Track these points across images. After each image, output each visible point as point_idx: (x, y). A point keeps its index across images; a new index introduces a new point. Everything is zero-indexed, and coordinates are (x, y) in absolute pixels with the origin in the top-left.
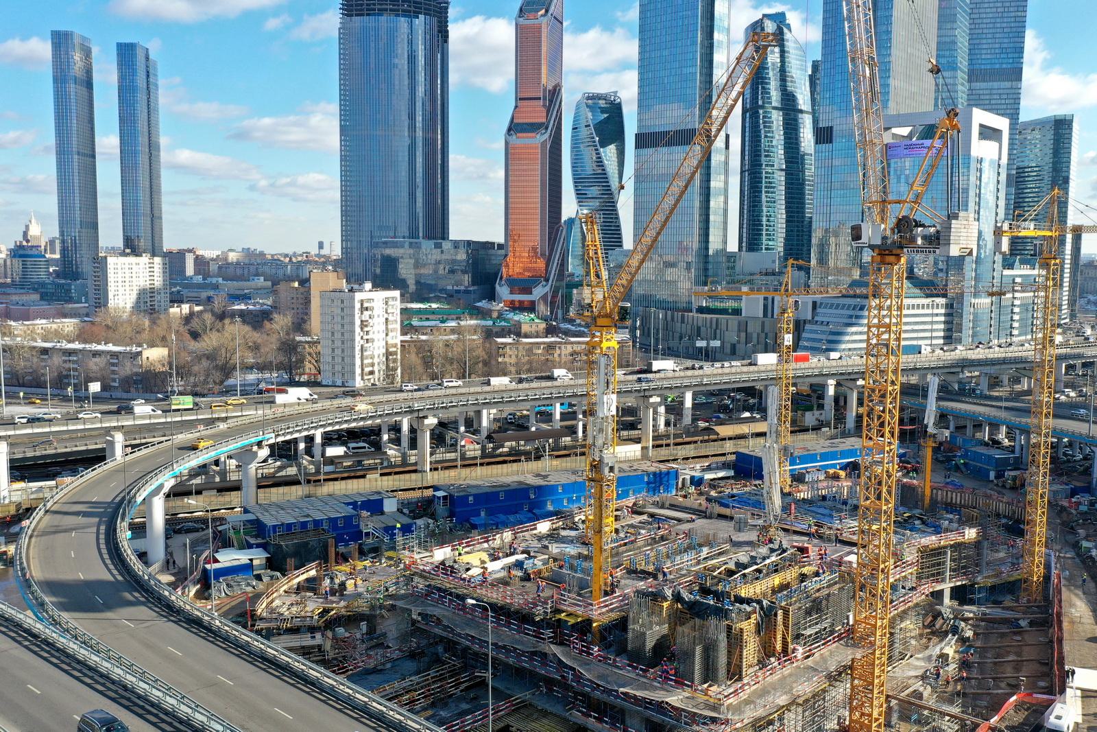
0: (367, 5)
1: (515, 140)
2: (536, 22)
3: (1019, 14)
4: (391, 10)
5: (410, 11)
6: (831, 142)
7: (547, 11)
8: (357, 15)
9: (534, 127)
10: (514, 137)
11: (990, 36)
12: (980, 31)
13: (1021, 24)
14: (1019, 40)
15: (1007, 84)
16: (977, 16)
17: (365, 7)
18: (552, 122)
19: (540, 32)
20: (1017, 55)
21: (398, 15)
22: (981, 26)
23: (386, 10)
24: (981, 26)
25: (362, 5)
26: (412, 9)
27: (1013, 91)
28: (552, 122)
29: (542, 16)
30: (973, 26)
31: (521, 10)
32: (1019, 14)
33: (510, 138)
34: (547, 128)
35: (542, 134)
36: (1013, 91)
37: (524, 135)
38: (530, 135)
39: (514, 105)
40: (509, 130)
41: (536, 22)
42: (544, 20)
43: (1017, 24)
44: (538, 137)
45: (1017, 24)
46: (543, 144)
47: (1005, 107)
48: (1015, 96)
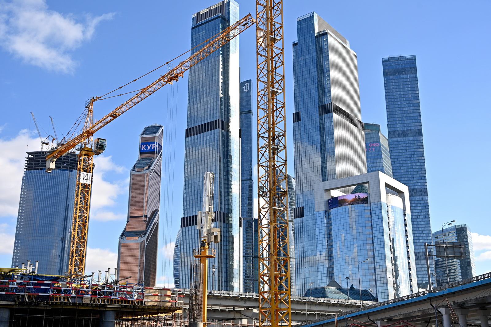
0: (42, 164)
2: (142, 173)
3: (420, 158)
5: (67, 168)
6: (303, 216)
7: (149, 167)
8: (34, 169)
9: (137, 234)
10: (125, 239)
11: (405, 171)
12: (399, 168)
13: (422, 164)
14: (423, 172)
15: (420, 198)
16: (396, 160)
17: (40, 165)
19: (144, 179)
20: (422, 181)
21: (60, 169)
22: (399, 165)
24: (399, 165)
25: (39, 164)
26: (69, 166)
27: (424, 202)
29: (146, 169)
30: (395, 165)
31: (134, 167)
32: (420, 158)
33: (122, 240)
34: (145, 234)
35: (142, 237)
36: (424, 202)
37: (131, 238)
41: (142, 173)
42: (147, 171)
43: (420, 164)
44: (139, 239)
45: (420, 164)
46: (142, 243)
47: (420, 211)
48: (425, 205)
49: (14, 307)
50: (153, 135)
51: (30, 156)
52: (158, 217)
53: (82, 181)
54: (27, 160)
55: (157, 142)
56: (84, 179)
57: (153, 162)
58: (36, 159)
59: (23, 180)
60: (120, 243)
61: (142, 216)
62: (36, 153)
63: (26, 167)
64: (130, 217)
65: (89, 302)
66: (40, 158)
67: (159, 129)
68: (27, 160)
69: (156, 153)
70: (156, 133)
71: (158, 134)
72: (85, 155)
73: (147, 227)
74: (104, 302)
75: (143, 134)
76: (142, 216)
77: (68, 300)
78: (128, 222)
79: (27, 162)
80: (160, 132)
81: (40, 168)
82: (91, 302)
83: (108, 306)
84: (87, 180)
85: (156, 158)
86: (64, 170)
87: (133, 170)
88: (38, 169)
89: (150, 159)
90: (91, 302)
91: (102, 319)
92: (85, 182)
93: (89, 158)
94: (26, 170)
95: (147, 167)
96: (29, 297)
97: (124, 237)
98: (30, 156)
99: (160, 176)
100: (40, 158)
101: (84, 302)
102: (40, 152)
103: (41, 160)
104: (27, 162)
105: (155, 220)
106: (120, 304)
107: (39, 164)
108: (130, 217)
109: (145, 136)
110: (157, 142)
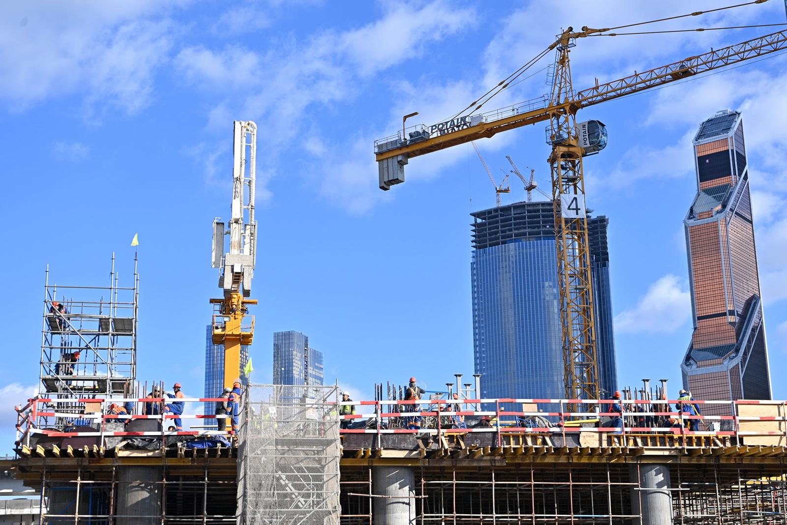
0: (502, 232)
1: (694, 370)
2: (710, 220)
4: (530, 234)
7: (724, 206)
8: (491, 245)
9: (720, 352)
10: (694, 367)
18: (745, 343)
21: (540, 238)
23: (525, 234)
28: (745, 343)
29: (718, 212)
34: (737, 351)
35: (731, 359)
38: (717, 361)
39: (692, 326)
40: (688, 358)
44: (726, 363)
46: (734, 371)
49: (420, 464)
50: (722, 136)
51: (479, 221)
52: (760, 312)
53: (564, 216)
54: (474, 228)
55: (732, 151)
56: (569, 208)
57: (731, 193)
58: (489, 224)
59: (473, 269)
60: (684, 375)
61: (724, 314)
62: (490, 212)
63: (474, 244)
64: (700, 318)
65: (596, 445)
66: (497, 222)
67: (733, 121)
68: (474, 228)
69: (735, 174)
70: (728, 129)
71: (731, 133)
72: (563, 156)
73: (738, 335)
74: (636, 443)
75: (699, 137)
76: (724, 314)
77: (544, 442)
78: (695, 329)
79: (474, 233)
80: (736, 126)
81: (501, 240)
82: (601, 444)
83: (647, 453)
84: (577, 209)
85: (737, 183)
86: (548, 238)
87: (689, 218)
88: (498, 244)
89: (725, 188)
90: (601, 444)
91: (637, 486)
92: (572, 215)
93: (573, 162)
94: (474, 249)
95: (719, 207)
96: (451, 438)
97: (692, 361)
98: (479, 221)
99: (751, 222)
100: (497, 222)
101: (583, 446)
102: (496, 210)
103: (500, 224)
104: (474, 233)
105: (755, 320)
106: (677, 445)
107: (497, 232)
108: (700, 318)
109: (703, 141)
110: (732, 151)
